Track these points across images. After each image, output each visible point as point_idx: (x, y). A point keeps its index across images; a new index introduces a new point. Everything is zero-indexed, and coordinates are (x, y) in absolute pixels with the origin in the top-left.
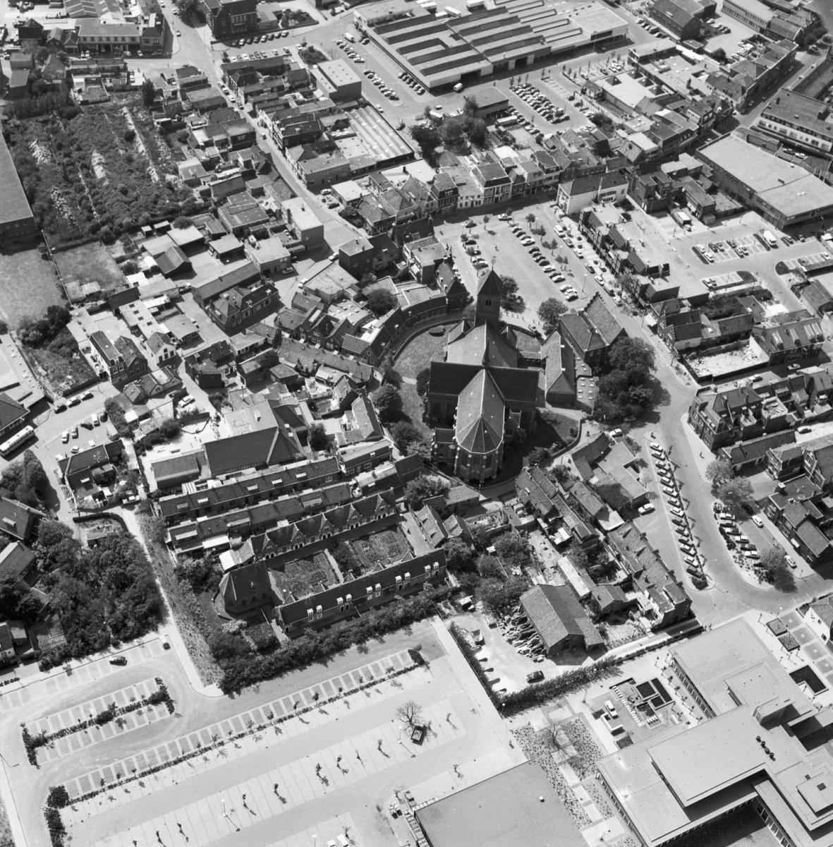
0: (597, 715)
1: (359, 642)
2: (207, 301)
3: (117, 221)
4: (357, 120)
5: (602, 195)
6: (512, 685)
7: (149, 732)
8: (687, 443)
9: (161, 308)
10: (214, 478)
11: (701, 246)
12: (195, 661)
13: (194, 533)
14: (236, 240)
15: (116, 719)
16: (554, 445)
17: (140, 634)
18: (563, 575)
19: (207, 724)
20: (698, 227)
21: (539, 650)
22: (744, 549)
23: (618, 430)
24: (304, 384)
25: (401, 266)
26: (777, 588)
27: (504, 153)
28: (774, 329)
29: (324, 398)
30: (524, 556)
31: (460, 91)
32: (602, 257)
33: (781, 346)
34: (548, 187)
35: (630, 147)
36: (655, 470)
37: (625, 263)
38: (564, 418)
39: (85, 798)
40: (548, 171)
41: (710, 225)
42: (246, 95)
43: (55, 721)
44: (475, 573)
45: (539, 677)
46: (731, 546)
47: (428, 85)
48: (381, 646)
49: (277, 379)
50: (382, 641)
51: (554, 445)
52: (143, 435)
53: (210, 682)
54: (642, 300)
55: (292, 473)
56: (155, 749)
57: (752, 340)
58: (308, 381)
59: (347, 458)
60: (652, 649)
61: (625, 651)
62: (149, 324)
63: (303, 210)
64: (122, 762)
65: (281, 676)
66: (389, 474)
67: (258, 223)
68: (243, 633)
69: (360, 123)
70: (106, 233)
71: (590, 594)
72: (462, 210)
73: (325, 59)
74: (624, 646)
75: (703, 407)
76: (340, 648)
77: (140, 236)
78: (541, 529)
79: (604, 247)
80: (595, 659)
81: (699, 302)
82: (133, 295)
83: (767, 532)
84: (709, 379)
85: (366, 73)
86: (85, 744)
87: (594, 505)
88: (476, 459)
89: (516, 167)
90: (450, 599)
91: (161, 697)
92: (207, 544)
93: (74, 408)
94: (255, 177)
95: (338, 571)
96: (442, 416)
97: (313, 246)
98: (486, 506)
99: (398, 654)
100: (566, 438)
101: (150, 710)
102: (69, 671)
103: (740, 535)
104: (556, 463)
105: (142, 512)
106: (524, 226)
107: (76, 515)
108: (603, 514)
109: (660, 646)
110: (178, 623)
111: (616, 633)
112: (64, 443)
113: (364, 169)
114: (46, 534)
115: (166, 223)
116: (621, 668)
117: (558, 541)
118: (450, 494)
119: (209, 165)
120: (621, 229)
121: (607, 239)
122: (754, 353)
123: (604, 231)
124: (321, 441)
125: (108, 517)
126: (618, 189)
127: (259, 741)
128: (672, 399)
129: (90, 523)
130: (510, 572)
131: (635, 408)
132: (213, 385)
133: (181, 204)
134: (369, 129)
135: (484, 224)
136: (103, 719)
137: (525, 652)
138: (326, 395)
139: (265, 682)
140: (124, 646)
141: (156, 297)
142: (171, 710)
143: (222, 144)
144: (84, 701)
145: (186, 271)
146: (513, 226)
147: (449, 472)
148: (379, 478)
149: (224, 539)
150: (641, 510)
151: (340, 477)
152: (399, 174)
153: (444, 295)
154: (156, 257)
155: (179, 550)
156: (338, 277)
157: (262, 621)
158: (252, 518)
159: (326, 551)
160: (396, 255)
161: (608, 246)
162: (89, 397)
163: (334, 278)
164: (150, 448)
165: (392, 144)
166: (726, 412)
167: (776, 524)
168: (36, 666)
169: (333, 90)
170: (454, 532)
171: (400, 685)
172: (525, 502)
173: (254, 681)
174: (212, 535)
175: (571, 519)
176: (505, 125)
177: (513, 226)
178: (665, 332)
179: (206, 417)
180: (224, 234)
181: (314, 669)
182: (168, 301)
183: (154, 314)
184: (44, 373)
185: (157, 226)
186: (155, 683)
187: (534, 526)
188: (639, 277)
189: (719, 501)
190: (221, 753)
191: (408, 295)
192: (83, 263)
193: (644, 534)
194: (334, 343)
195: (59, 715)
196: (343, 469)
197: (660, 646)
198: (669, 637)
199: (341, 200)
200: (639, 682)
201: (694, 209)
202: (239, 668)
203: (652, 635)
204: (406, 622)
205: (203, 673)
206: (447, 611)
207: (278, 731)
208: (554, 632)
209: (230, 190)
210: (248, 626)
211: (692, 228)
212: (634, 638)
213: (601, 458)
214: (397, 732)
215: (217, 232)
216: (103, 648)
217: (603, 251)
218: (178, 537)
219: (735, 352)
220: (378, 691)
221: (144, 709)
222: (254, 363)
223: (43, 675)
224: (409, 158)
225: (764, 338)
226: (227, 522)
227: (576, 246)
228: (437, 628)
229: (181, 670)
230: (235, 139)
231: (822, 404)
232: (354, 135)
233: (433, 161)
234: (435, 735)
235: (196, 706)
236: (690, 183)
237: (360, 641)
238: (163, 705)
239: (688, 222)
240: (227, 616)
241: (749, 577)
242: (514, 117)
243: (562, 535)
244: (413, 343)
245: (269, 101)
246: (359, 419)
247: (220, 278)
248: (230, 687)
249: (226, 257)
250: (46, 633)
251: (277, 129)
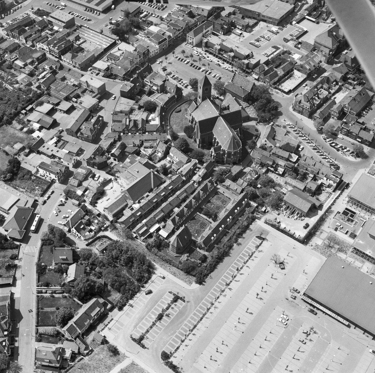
0: (336, 229)
1: (235, 243)
2: (76, 132)
3: (7, 113)
4: (81, 34)
5: (206, 33)
6: (302, 233)
7: (181, 313)
9: (56, 143)
10: (134, 203)
11: (253, 41)
12: (179, 278)
13: (145, 228)
14: (67, 103)
15: (165, 315)
16: (254, 138)
17: (149, 278)
18: (291, 185)
19: (202, 299)
20: (245, 34)
21: (302, 215)
22: (343, 149)
23: (272, 123)
24: (141, 151)
25: (147, 89)
26: (362, 158)
27: (153, 29)
28: (305, 64)
29: (153, 154)
30: (270, 183)
31: (115, 8)
32: (220, 58)
33: (310, 70)
34: (179, 37)
35: (203, 10)
36: (294, 133)
37: (234, 57)
38: (249, 126)
39: (176, 350)
40: (179, 30)
41: (250, 32)
42: (26, 39)
43: (140, 327)
44: (260, 197)
45: (307, 226)
46: (338, 150)
47: (101, 10)
48: (244, 240)
49: (130, 153)
50: (244, 238)
51: (254, 138)
52: (91, 199)
53: (191, 283)
54: (248, 70)
55: (167, 188)
56: (189, 319)
57: (295, 71)
58: (142, 149)
59: (184, 173)
60: (337, 198)
61: (329, 203)
62: (58, 151)
63: (92, 79)
64: (180, 330)
65: (216, 268)
66: (204, 172)
67: (73, 92)
68: (189, 258)
69: (84, 35)
70: (7, 120)
71: (305, 187)
72: (154, 57)
73: (50, 13)
75: (300, 102)
76: (231, 247)
77: (22, 116)
78: (271, 171)
79: (219, 54)
80: (321, 210)
81: (267, 63)
82: (41, 142)
83: (346, 140)
84: (290, 92)
85: (69, 13)
86: (160, 331)
87: (286, 154)
88: (235, 153)
89: (165, 33)
90: (257, 211)
91: (176, 299)
92: (152, 230)
93: (49, 200)
94: (58, 73)
95: (208, 219)
96: (208, 142)
97: (103, 94)
98: (244, 171)
99: (253, 240)
100: (255, 133)
101: (176, 305)
102: (131, 306)
103: (338, 145)
104: (259, 145)
105: (113, 230)
106: (181, 56)
107: (87, 243)
108: (290, 156)
109: (339, 196)
111: (322, 197)
112: (56, 216)
113: (100, 54)
114: (84, 255)
115: (30, 107)
116: (332, 209)
117: (281, 173)
118: (232, 171)
119: (31, 74)
120: (224, 43)
121: (220, 50)
122: (298, 76)
123: (219, 47)
124: (166, 171)
125: (99, 238)
126: (209, 29)
127: (226, 296)
128: (282, 104)
129: (94, 244)
130: (271, 192)
131: (273, 112)
132: (104, 166)
133: (31, 95)
134: (90, 36)
135: (165, 60)
136: (160, 317)
137: (297, 219)
138: (153, 152)
139: (212, 273)
140: (146, 285)
141: (51, 139)
142: (184, 301)
143: (32, 63)
144: (146, 314)
145: (55, 124)
146: (177, 58)
147: (223, 163)
148: (202, 176)
149: (157, 226)
150: (300, 149)
151: (184, 183)
152: (117, 51)
153: (174, 94)
154: (38, 122)
155: (143, 238)
156: (125, 103)
157: (193, 250)
158: (164, 212)
159: (198, 213)
160: (142, 85)
161: (221, 53)
162: (53, 192)
163: (125, 104)
164: (97, 203)
165: (104, 40)
166: (309, 101)
167: (348, 136)
168: (116, 310)
169: (64, 24)
170: (243, 185)
171: (262, 251)
172: (260, 163)
173: (208, 275)
174: (152, 226)
175: (282, 163)
176: (144, 17)
177: (177, 58)
178: (264, 79)
179: (110, 181)
180: (60, 102)
181: (226, 259)
182: (58, 139)
183: (56, 146)
184: (24, 190)
185: (28, 109)
186: (170, 294)
187: (268, 171)
188: (243, 61)
189: (324, 135)
190: (215, 307)
191: (160, 99)
192: (4, 137)
193: (312, 157)
194: (142, 130)
195: (140, 324)
196: (184, 178)
197: (339, 196)
198: (340, 192)
199: (100, 70)
200: (342, 212)
201: (240, 28)
202: (199, 273)
203: (334, 193)
204: (247, 227)
205: (186, 282)
206: (259, 216)
207: (230, 289)
208: (305, 207)
209: (49, 82)
210: (190, 255)
211: (244, 35)
212: (329, 197)
213: (275, 136)
214: (274, 269)
215: (57, 102)
216: (139, 291)
217: (220, 56)
218: (140, 232)
219: (291, 78)
220: (255, 257)
221: (173, 306)
222: (118, 150)
223: (121, 313)
224: (114, 45)
225: (301, 69)
226: (155, 218)
227: (206, 57)
228: (260, 224)
229: (176, 284)
230: (38, 59)
231: (335, 86)
232: (85, 41)
233: (126, 41)
234: (287, 263)
235: (192, 294)
236: (234, 18)
237: (236, 241)
238: (179, 301)
239: (241, 34)
240: (178, 255)
241: (351, 159)
242: (145, 13)
243: (281, 170)
244: (172, 119)
245: (38, 38)
246: (176, 156)
247: (77, 121)
248: (200, 281)
249: (69, 111)
250: (110, 296)
251: (53, 49)
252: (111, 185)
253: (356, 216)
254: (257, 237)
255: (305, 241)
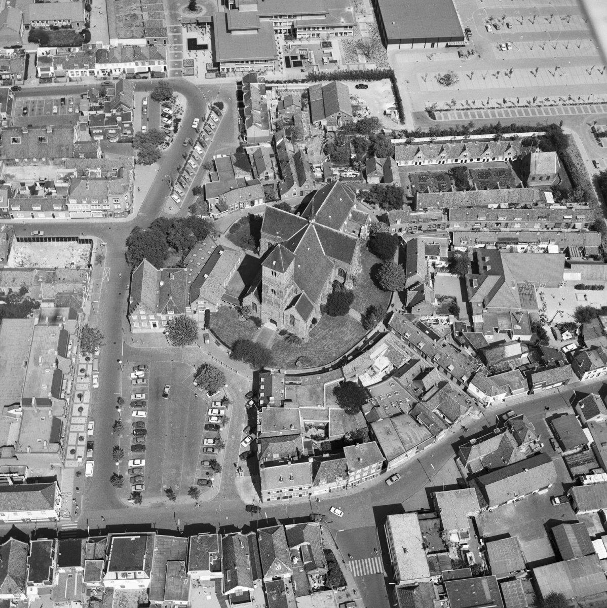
8: (146, 200)
46: (179, 120)
74: (294, 88)
109: (272, 82)
110: (586, 173)
156: (393, 437)
197: (272, 82)
227: (84, 443)
229: (586, 147)
252: (559, 320)
253: (289, 55)
254: (434, 118)
255: (390, 75)
